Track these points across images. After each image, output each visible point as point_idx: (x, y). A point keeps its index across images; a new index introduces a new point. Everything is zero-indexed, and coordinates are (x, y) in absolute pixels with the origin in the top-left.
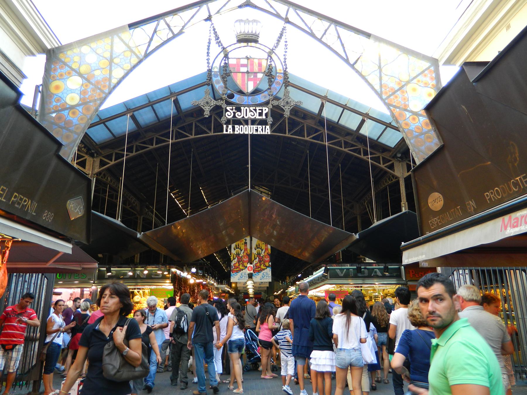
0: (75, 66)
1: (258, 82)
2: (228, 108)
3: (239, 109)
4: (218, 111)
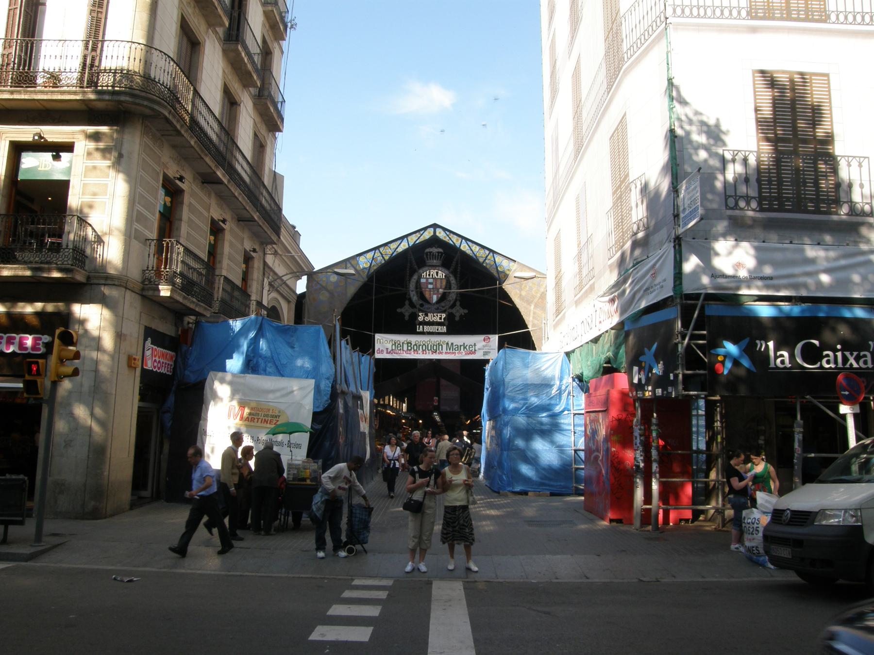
0: (324, 285)
1: (440, 296)
2: (420, 314)
3: (427, 315)
4: (414, 316)
